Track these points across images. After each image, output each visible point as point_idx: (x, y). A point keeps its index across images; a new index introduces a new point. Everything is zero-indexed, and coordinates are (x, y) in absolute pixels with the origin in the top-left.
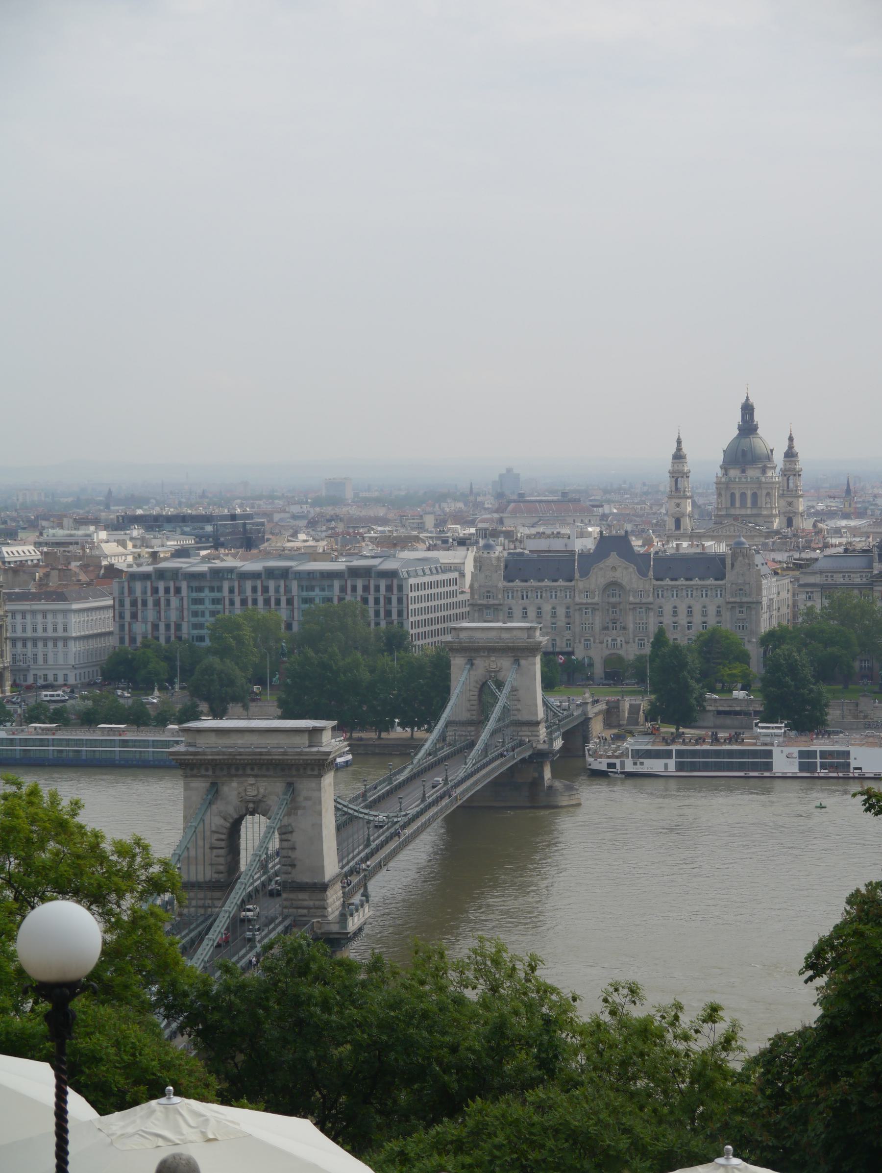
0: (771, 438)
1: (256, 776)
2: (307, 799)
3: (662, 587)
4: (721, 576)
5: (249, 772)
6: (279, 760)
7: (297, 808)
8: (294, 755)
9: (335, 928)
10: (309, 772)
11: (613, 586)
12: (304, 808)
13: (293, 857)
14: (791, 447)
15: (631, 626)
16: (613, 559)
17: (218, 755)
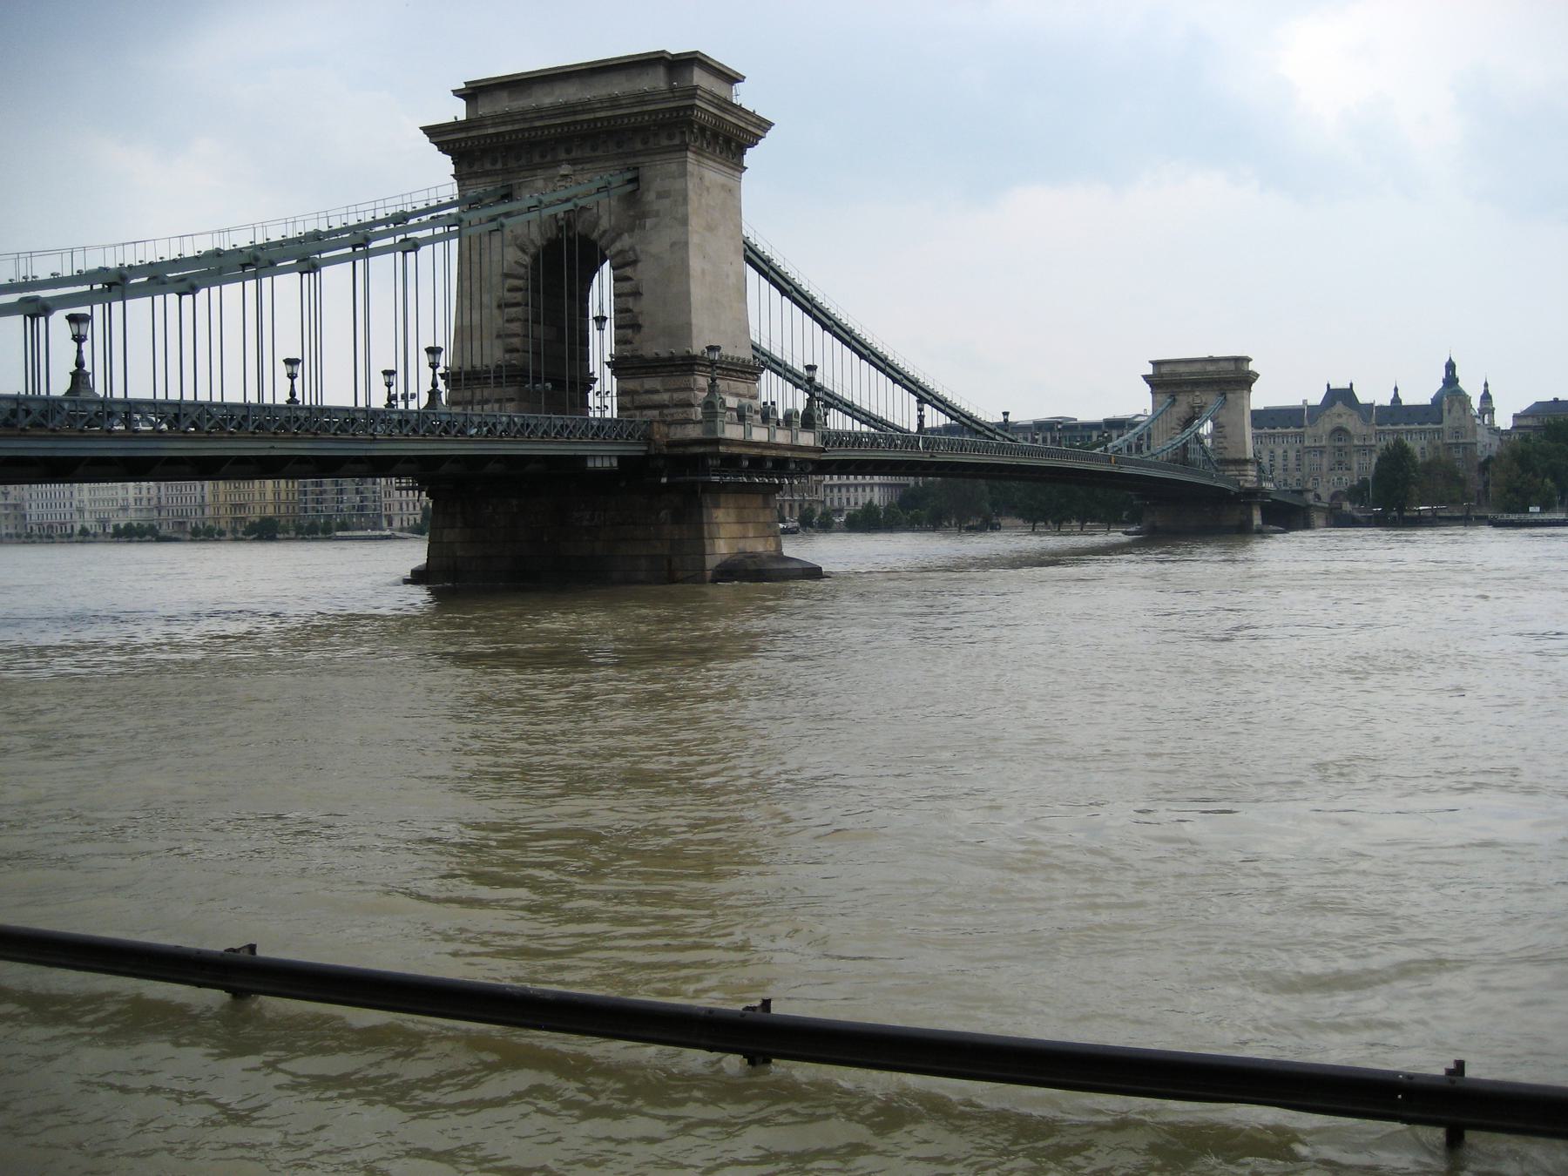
0: (1471, 387)
1: (573, 162)
2: (660, 196)
3: (1383, 432)
4: (1440, 422)
5: (563, 156)
6: (608, 119)
7: (643, 215)
8: (633, 105)
9: (694, 432)
10: (665, 142)
11: (1340, 432)
12: (657, 214)
13: (636, 310)
14: (1486, 392)
15: (1355, 466)
16: (1339, 407)
17: (504, 123)
